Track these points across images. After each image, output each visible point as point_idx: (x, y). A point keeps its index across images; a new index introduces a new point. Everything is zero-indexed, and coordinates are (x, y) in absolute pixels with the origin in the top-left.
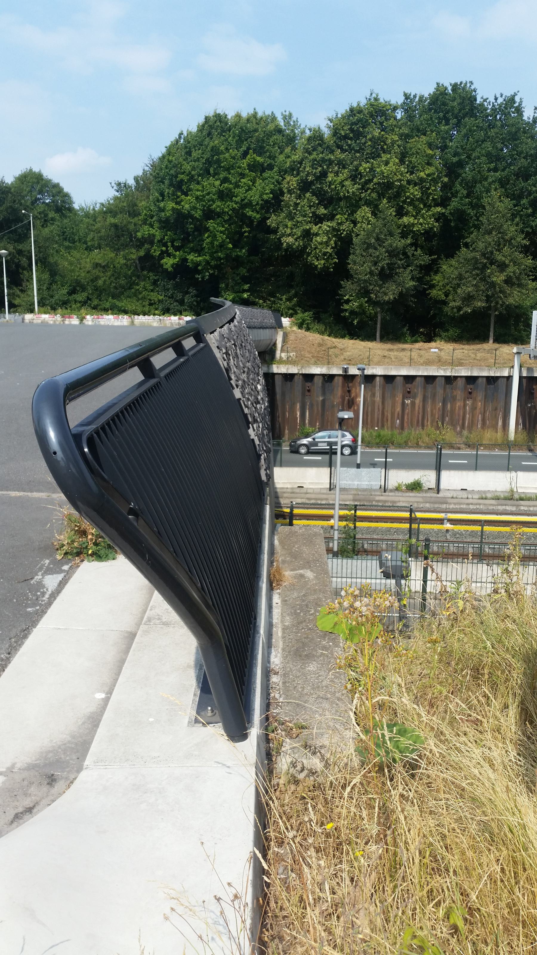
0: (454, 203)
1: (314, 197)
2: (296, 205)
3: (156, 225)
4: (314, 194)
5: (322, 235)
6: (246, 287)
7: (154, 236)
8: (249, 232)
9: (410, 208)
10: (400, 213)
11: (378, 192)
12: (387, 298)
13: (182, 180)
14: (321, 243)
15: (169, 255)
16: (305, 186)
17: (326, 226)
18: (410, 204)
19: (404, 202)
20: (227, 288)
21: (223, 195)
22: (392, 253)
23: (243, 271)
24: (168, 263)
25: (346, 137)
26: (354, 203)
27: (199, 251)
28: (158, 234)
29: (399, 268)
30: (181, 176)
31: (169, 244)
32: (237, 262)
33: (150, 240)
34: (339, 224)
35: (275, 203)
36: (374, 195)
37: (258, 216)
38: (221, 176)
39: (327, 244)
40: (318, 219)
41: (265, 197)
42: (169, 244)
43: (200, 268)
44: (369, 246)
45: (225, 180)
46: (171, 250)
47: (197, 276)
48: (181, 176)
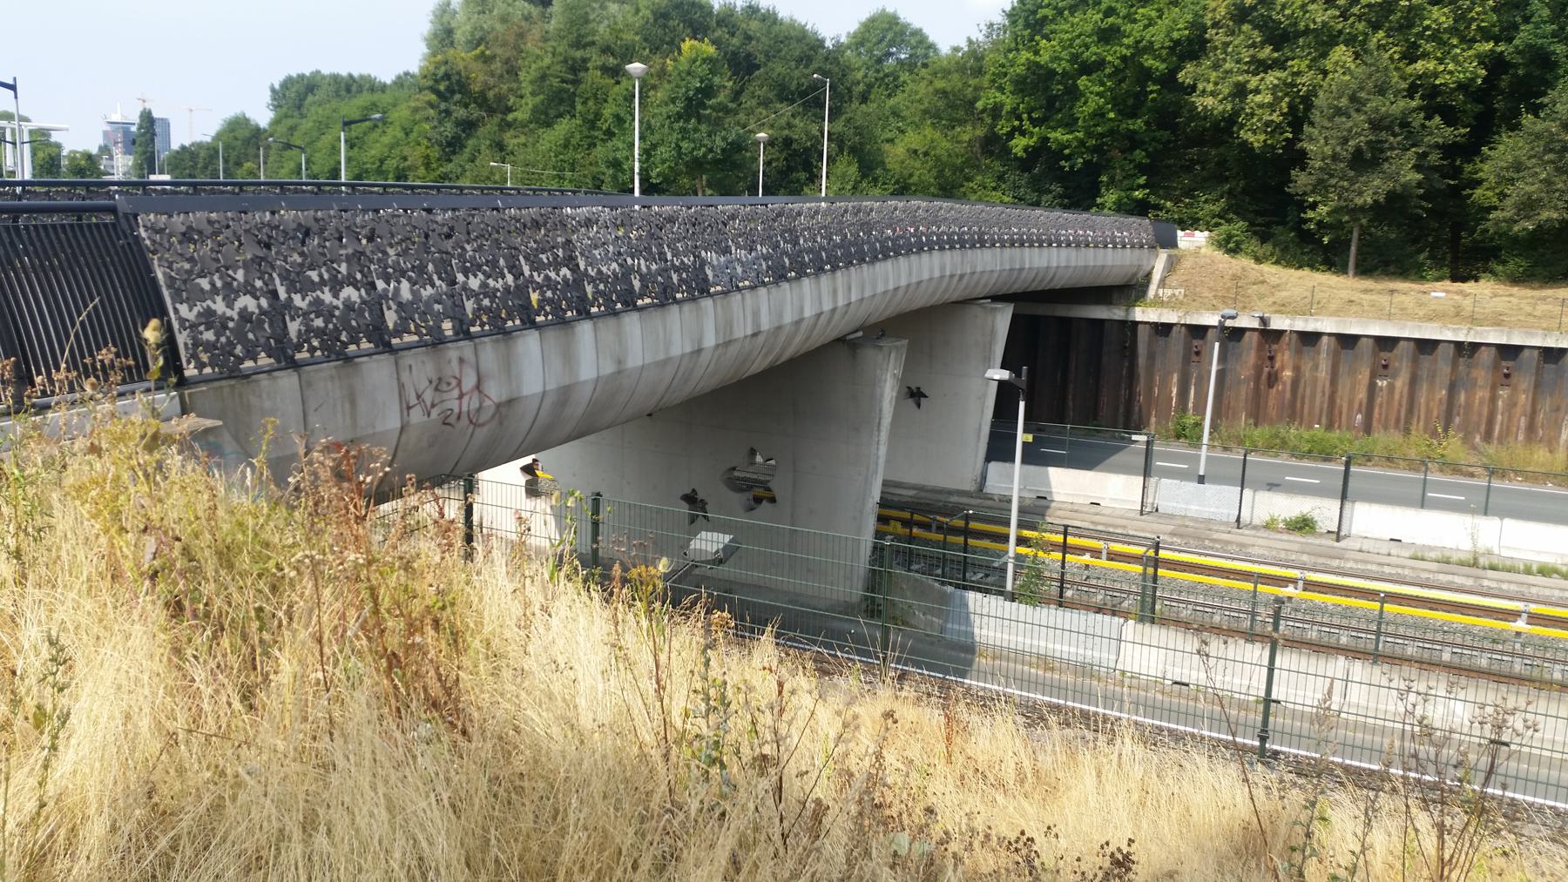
0: (1524, 35)
1: (1256, 32)
2: (1227, 44)
3: (1009, 88)
6: (1142, 180)
7: (1002, 105)
8: (1158, 92)
9: (1429, 47)
10: (1411, 56)
11: (1369, 21)
12: (1359, 201)
13: (1045, 17)
14: (1261, 106)
15: (1023, 133)
17: (1272, 78)
18: (1433, 38)
19: (1420, 35)
20: (1112, 182)
21: (1108, 35)
22: (1377, 125)
23: (1139, 154)
24: (1019, 144)
26: (1326, 40)
27: (1070, 124)
28: (1008, 101)
29: (1392, 148)
31: (1025, 116)
32: (1133, 141)
33: (996, 111)
35: (1193, 47)
37: (1163, 66)
39: (1272, 107)
40: (1262, 66)
41: (1176, 35)
42: (1025, 116)
43: (1067, 151)
46: (1026, 124)
47: (1063, 163)
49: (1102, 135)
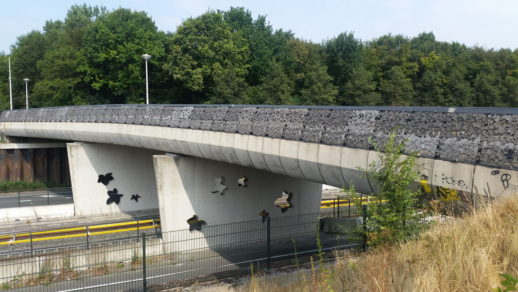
4: (190, 54)
5: (198, 75)
7: (87, 71)
15: (96, 82)
16: (185, 50)
17: (199, 70)
18: (237, 62)
24: (96, 86)
25: (203, 29)
30: (110, 41)
33: (85, 73)
34: (205, 69)
36: (222, 57)
38: (136, 42)
40: (193, 68)
41: (162, 54)
42: (96, 76)
44: (227, 81)
45: (138, 44)
47: (114, 93)
48: (110, 41)
49: (129, 84)
